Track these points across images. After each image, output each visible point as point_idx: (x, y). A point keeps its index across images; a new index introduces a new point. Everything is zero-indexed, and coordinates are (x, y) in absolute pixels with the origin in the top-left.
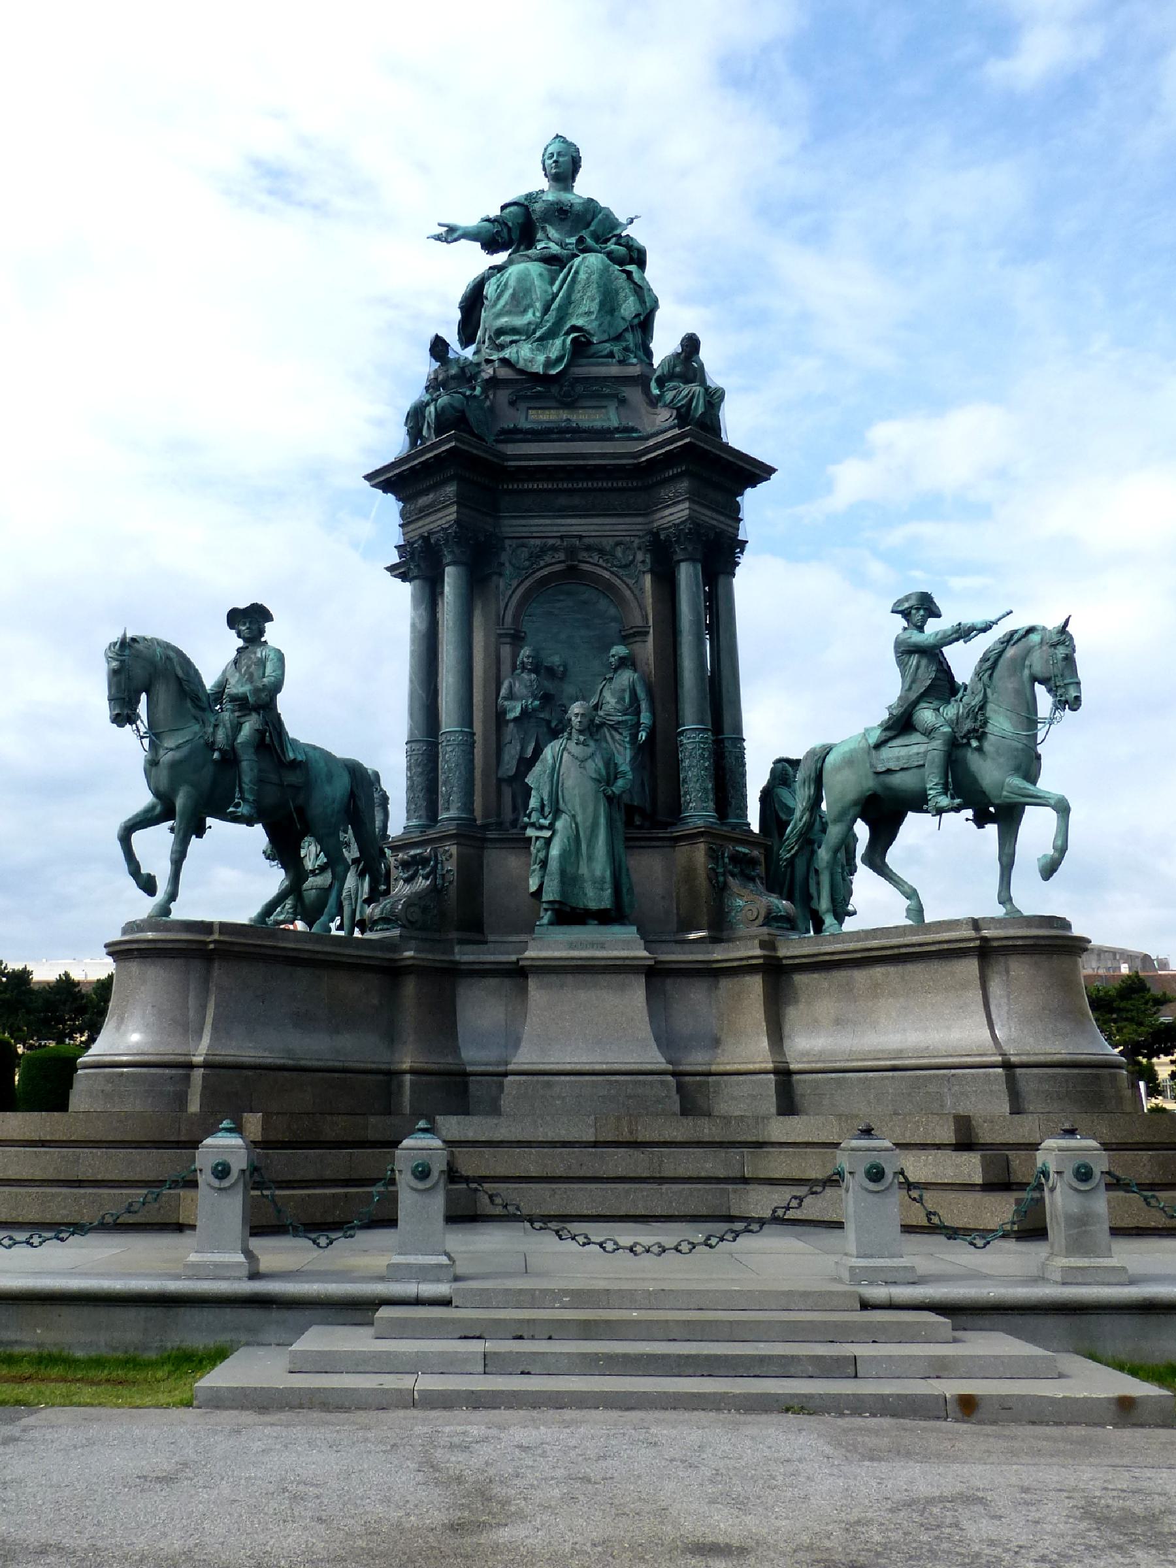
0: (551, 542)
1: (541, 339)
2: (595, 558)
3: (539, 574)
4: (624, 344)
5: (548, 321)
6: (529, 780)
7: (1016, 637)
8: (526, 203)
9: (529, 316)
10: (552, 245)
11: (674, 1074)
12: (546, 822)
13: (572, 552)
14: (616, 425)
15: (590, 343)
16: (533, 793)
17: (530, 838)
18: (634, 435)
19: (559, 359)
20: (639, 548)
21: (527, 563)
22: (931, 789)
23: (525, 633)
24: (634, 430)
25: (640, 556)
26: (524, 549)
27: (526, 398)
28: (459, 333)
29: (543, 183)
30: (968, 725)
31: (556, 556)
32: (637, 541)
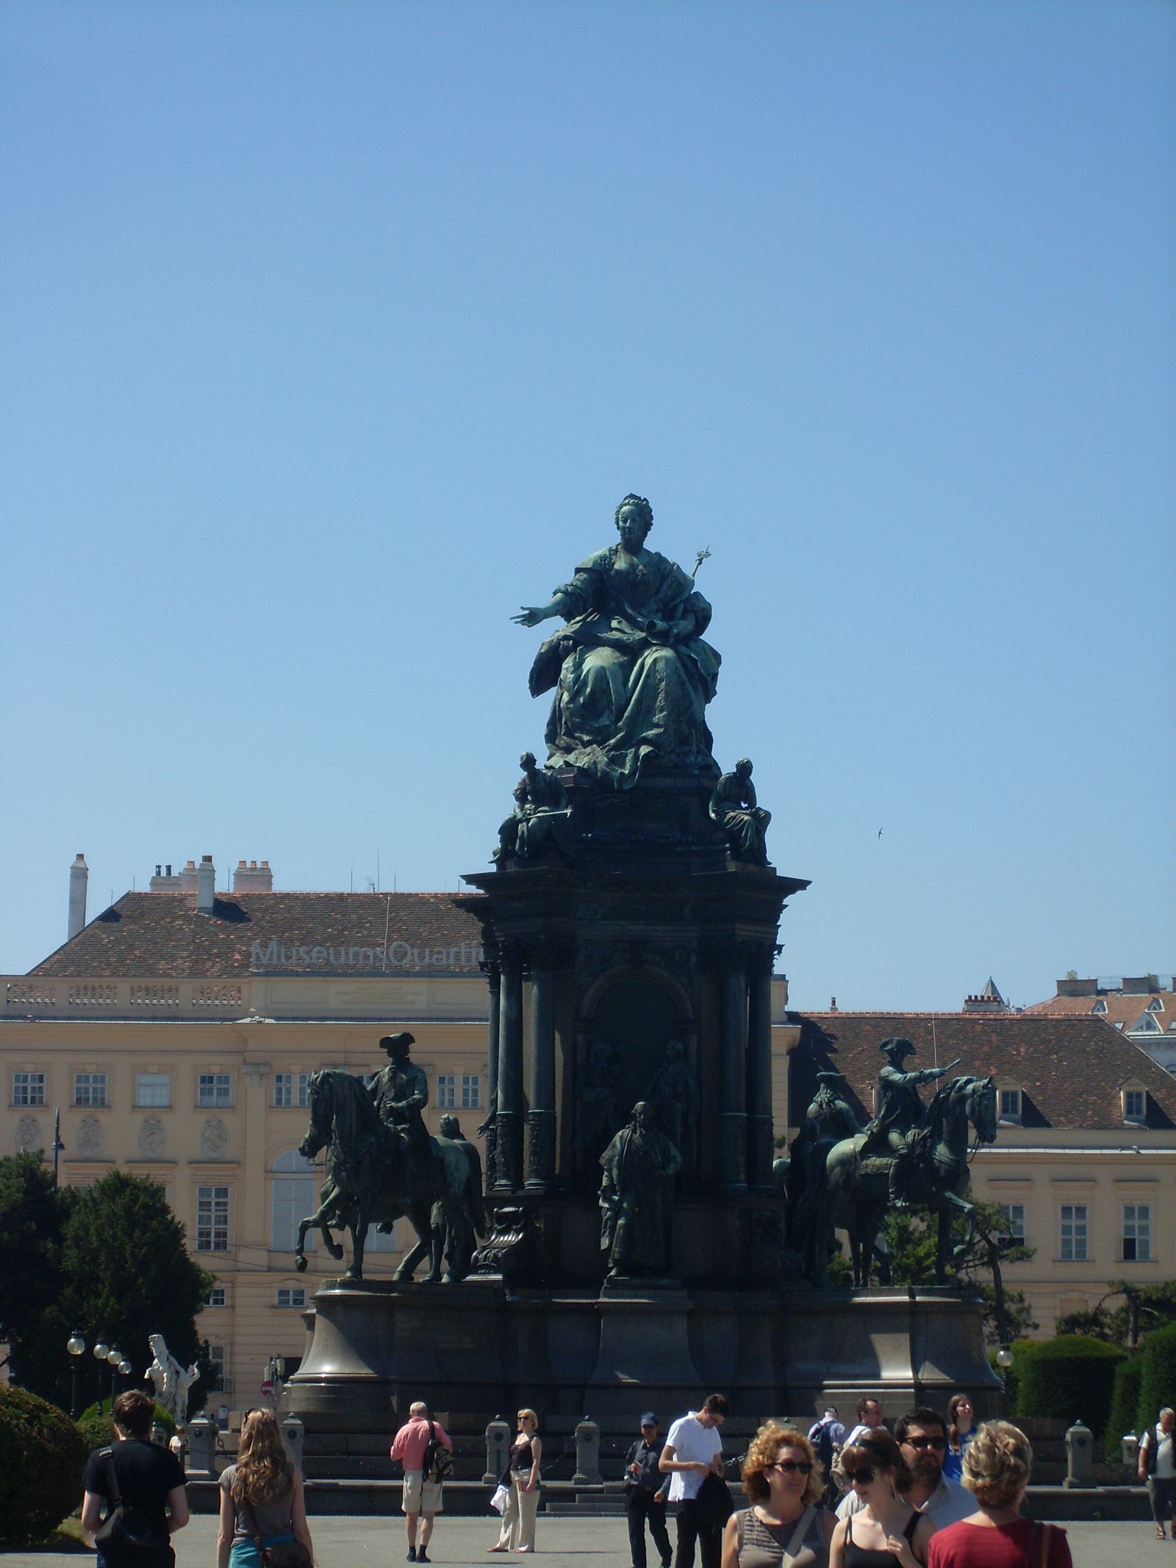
1: (615, 747)
4: (687, 748)
5: (620, 730)
6: (602, 1161)
7: (958, 1084)
8: (600, 569)
9: (605, 720)
10: (625, 626)
12: (616, 1198)
15: (657, 756)
16: (606, 1173)
17: (602, 1207)
18: (693, 848)
19: (632, 773)
22: (892, 1193)
25: (693, 960)
28: (531, 681)
29: (616, 538)
30: (918, 1150)
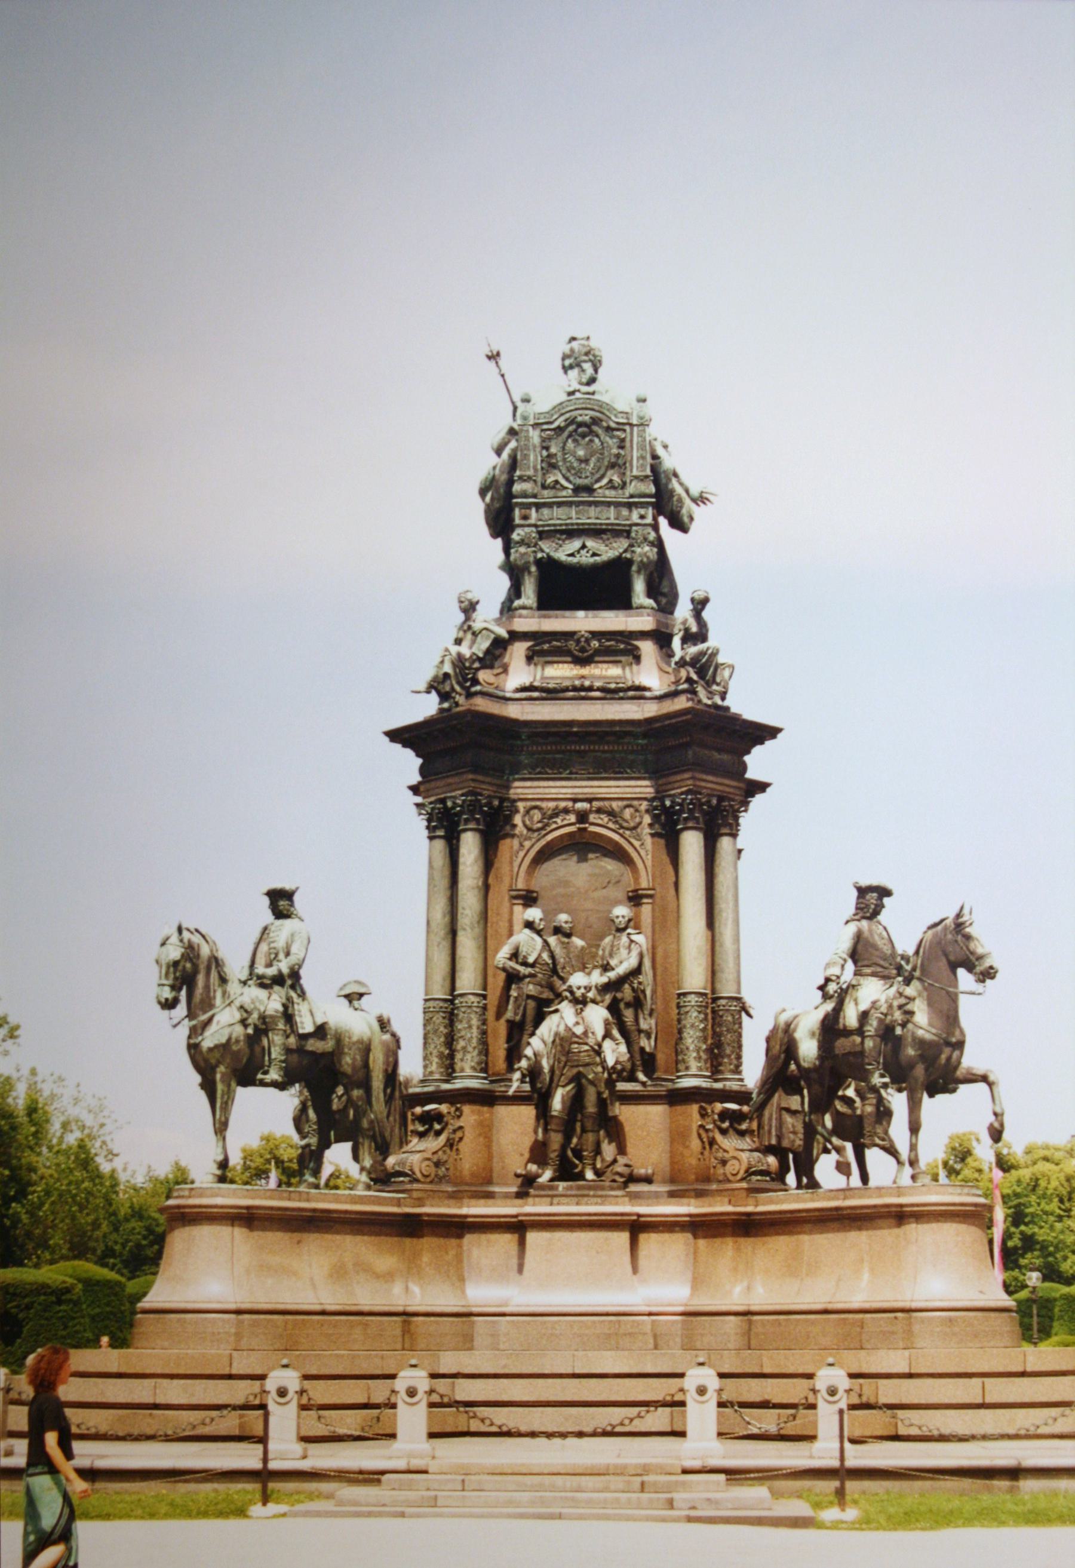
0: (562, 804)
2: (604, 819)
3: (549, 837)
11: (650, 1314)
13: (582, 817)
14: (630, 684)
18: (647, 694)
20: (647, 811)
21: (540, 825)
23: (537, 892)
24: (645, 689)
25: (647, 819)
26: (536, 811)
27: (542, 653)
31: (568, 817)
32: (644, 805)
